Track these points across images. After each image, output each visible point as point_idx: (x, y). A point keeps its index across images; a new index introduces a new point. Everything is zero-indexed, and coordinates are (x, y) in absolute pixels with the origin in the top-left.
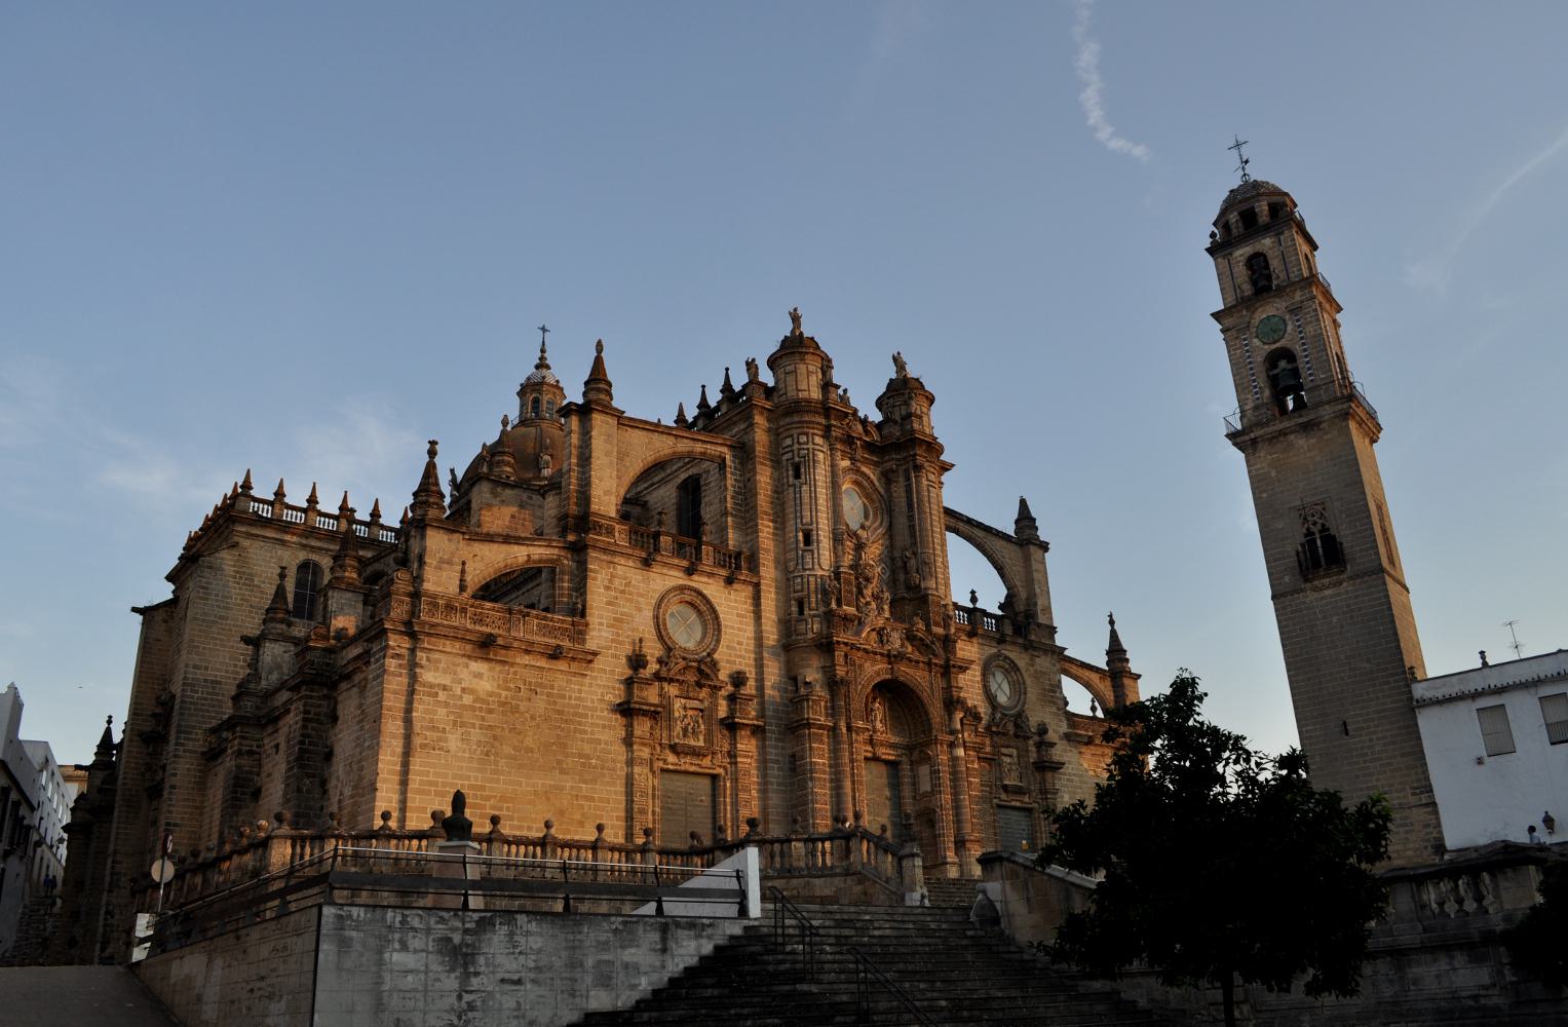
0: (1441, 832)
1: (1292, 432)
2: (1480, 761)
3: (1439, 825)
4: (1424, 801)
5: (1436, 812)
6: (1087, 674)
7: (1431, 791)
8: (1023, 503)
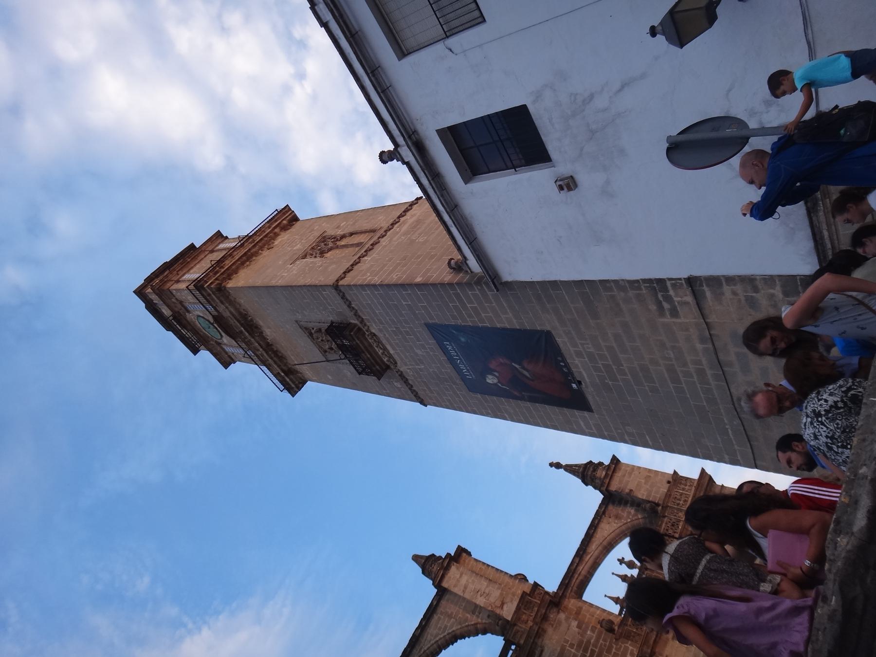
0: (770, 280)
1: (264, 339)
2: (568, 184)
3: (749, 281)
4: (689, 299)
5: (715, 281)
6: (594, 548)
7: (661, 282)
8: (416, 558)
